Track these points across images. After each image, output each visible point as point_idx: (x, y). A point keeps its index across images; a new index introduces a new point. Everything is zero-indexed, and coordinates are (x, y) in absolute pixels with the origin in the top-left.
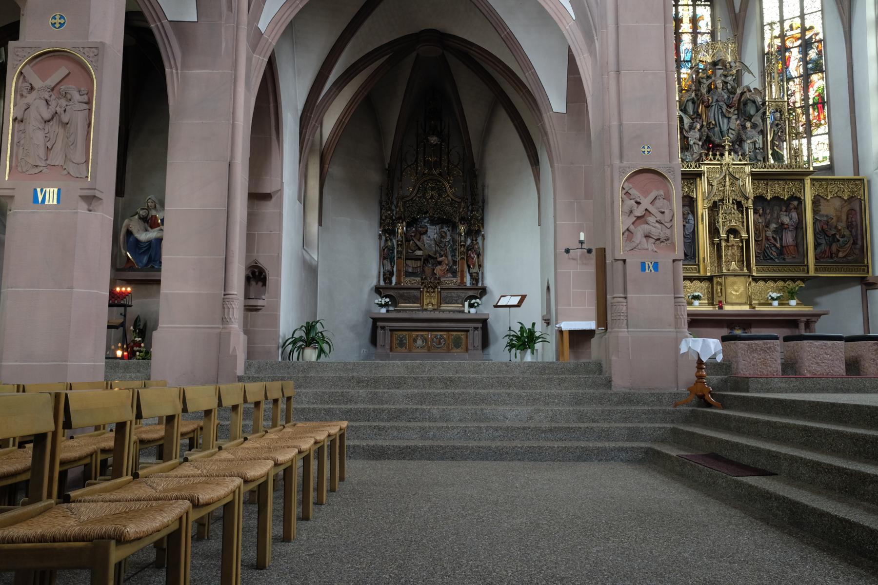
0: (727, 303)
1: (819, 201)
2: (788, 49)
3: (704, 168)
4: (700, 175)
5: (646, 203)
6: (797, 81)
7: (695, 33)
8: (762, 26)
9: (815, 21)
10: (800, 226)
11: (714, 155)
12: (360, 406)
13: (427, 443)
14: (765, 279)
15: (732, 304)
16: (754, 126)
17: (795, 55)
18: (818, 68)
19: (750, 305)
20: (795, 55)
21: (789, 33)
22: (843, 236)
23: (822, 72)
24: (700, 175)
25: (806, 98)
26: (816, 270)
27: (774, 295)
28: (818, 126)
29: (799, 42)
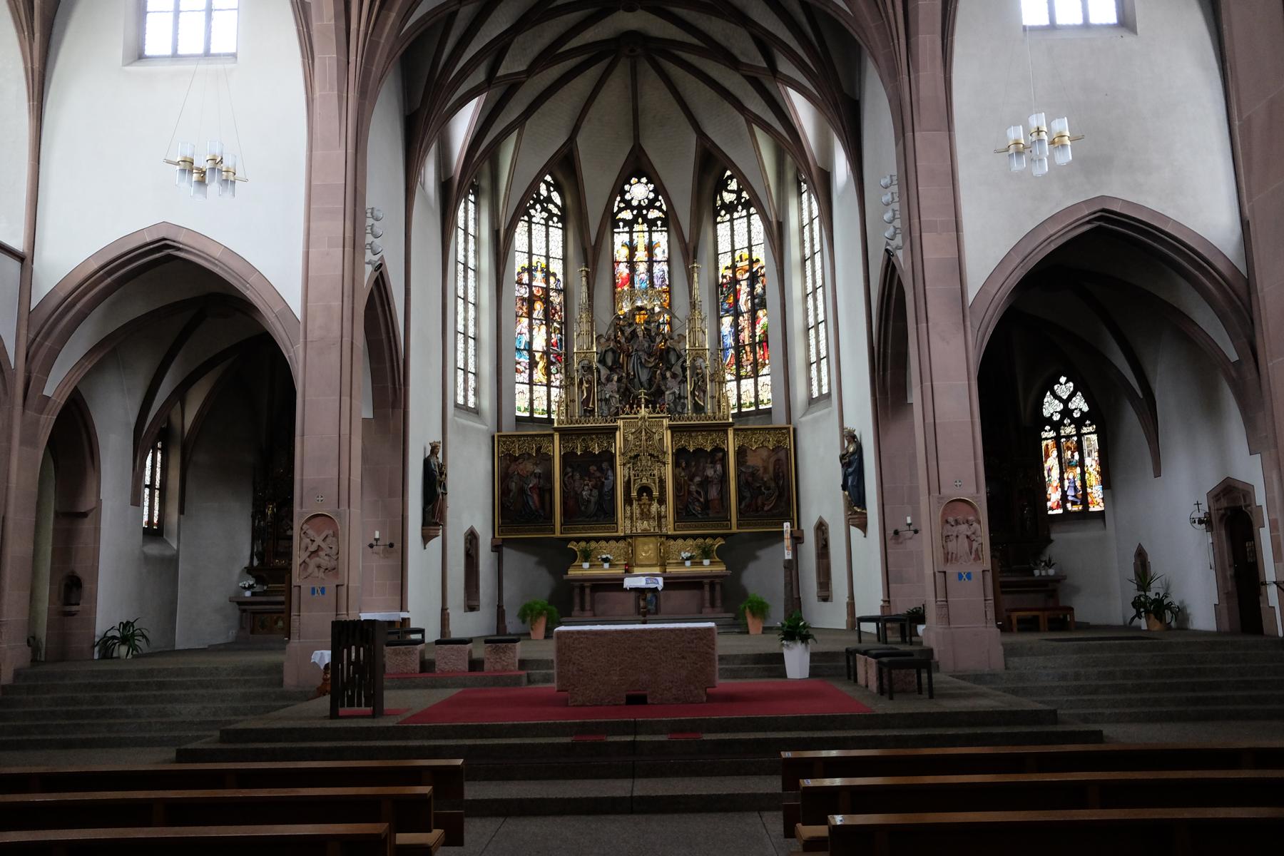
0: (638, 566)
1: (745, 451)
2: (737, 281)
3: (620, 423)
4: (616, 428)
5: (319, 541)
6: (746, 316)
7: (651, 261)
8: (717, 255)
9: (760, 253)
10: (724, 478)
11: (631, 408)
12: (85, 707)
13: (113, 735)
14: (685, 537)
15: (642, 566)
16: (674, 376)
17: (744, 287)
18: (763, 305)
19: (663, 565)
20: (744, 287)
21: (739, 265)
22: (768, 489)
23: (765, 307)
24: (616, 428)
25: (753, 335)
26: (739, 526)
27: (685, 555)
28: (764, 365)
29: (747, 275)
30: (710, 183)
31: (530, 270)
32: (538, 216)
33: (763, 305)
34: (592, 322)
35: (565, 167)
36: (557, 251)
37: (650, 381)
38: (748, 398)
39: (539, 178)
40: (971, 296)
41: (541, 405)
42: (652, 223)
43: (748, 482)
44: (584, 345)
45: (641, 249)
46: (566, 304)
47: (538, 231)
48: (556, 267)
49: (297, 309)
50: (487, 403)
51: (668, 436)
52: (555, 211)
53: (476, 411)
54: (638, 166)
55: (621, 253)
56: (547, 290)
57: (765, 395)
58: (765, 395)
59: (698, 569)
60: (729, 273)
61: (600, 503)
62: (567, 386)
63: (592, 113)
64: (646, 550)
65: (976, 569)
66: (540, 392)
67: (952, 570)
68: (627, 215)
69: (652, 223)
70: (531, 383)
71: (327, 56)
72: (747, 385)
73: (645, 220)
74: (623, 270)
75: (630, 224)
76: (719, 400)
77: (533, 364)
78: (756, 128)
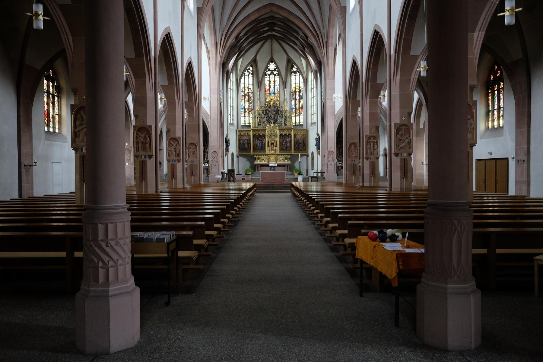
7: (275, 85)
9: (302, 85)
17: (297, 93)
18: (302, 98)
19: (276, 161)
20: (297, 93)
30: (290, 65)
31: (245, 88)
32: (246, 73)
33: (302, 98)
34: (260, 103)
35: (254, 62)
36: (251, 82)
38: (298, 121)
39: (248, 65)
40: (336, 112)
41: (247, 122)
42: (275, 75)
43: (297, 143)
44: (258, 108)
45: (272, 81)
47: (247, 77)
48: (251, 87)
49: (209, 113)
50: (235, 122)
51: (278, 131)
52: (251, 72)
53: (233, 124)
54: (272, 61)
55: (267, 83)
56: (249, 93)
57: (302, 121)
58: (302, 121)
59: (284, 162)
60: (294, 89)
61: (262, 147)
62: (254, 118)
63: (261, 50)
64: (272, 158)
65: (333, 163)
66: (247, 119)
67: (329, 163)
68: (269, 73)
69: (275, 75)
70: (245, 117)
71: (213, 61)
72: (298, 118)
73: (273, 74)
74: (267, 87)
75: (269, 75)
77: (245, 112)
78: (302, 59)
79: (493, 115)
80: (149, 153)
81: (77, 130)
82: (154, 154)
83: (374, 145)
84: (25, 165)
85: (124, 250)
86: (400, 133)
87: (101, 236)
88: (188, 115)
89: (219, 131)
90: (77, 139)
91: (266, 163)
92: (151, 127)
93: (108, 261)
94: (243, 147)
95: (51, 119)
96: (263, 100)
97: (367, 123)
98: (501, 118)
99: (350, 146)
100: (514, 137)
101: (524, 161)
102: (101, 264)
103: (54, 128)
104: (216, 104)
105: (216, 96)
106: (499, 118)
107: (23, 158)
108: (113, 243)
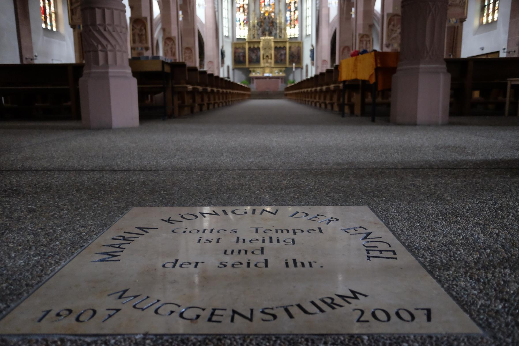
10: (285, 54)
34: (255, 14)
37: (269, 30)
43: (292, 56)
44: (253, 21)
46: (248, 8)
50: (230, 35)
53: (228, 37)
59: (279, 75)
62: (249, 30)
76: (285, 34)
79: (488, 9)
80: (145, 45)
81: (73, 7)
82: (150, 46)
83: (366, 44)
84: (26, 59)
85: (121, 37)
86: (392, 23)
87: (99, 21)
88: (183, 18)
89: (215, 40)
90: (74, 17)
91: (261, 75)
92: (146, 18)
93: (107, 45)
94: (238, 60)
95: (48, 17)
96: (258, 12)
97: (360, 21)
98: (496, 11)
99: (344, 49)
100: (507, 28)
101: (515, 52)
102: (100, 48)
103: (51, 25)
104: (210, 13)
105: (210, 5)
106: (494, 11)
107: (24, 52)
108: (110, 28)
